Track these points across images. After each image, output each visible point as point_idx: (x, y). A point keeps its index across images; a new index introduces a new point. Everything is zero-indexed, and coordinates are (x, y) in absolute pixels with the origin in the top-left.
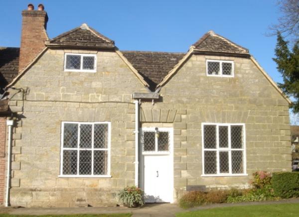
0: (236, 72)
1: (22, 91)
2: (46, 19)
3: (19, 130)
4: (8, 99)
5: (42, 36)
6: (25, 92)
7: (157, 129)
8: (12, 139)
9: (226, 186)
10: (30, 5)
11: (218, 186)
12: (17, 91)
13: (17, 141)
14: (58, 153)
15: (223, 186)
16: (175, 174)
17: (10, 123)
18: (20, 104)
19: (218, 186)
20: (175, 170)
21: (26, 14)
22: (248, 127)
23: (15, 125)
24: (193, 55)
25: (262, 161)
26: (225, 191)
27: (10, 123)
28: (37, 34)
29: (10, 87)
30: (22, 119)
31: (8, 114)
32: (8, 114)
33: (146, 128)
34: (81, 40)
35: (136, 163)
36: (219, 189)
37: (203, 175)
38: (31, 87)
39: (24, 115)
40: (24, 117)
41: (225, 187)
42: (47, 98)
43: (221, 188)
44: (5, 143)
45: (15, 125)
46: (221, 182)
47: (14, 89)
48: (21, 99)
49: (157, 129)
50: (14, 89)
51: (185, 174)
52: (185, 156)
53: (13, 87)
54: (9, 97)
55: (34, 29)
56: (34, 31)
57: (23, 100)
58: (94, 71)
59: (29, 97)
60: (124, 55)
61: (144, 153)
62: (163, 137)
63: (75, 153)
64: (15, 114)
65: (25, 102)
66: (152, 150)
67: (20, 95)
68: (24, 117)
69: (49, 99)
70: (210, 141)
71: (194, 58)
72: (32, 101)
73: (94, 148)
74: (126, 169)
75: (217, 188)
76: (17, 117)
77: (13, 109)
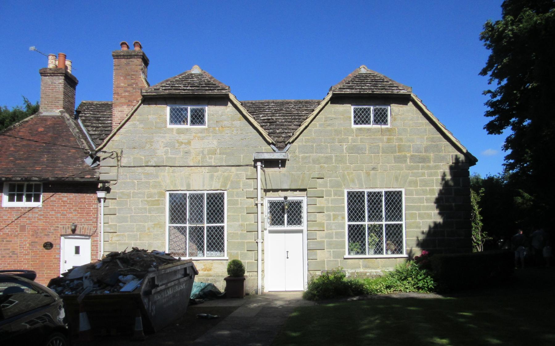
0: (394, 119)
1: (115, 155)
2: (146, 62)
5: (139, 83)
6: (118, 157)
7: (286, 198)
9: (379, 270)
10: (122, 44)
15: (373, 271)
21: (117, 57)
22: (408, 193)
28: (133, 81)
34: (187, 87)
36: (368, 274)
41: (376, 272)
42: (148, 162)
43: (371, 273)
44: (97, 220)
47: (105, 152)
49: (286, 198)
50: (105, 152)
55: (129, 75)
56: (128, 77)
58: (205, 127)
59: (124, 161)
60: (242, 105)
63: (202, 229)
66: (281, 224)
69: (150, 164)
70: (355, 212)
73: (208, 223)
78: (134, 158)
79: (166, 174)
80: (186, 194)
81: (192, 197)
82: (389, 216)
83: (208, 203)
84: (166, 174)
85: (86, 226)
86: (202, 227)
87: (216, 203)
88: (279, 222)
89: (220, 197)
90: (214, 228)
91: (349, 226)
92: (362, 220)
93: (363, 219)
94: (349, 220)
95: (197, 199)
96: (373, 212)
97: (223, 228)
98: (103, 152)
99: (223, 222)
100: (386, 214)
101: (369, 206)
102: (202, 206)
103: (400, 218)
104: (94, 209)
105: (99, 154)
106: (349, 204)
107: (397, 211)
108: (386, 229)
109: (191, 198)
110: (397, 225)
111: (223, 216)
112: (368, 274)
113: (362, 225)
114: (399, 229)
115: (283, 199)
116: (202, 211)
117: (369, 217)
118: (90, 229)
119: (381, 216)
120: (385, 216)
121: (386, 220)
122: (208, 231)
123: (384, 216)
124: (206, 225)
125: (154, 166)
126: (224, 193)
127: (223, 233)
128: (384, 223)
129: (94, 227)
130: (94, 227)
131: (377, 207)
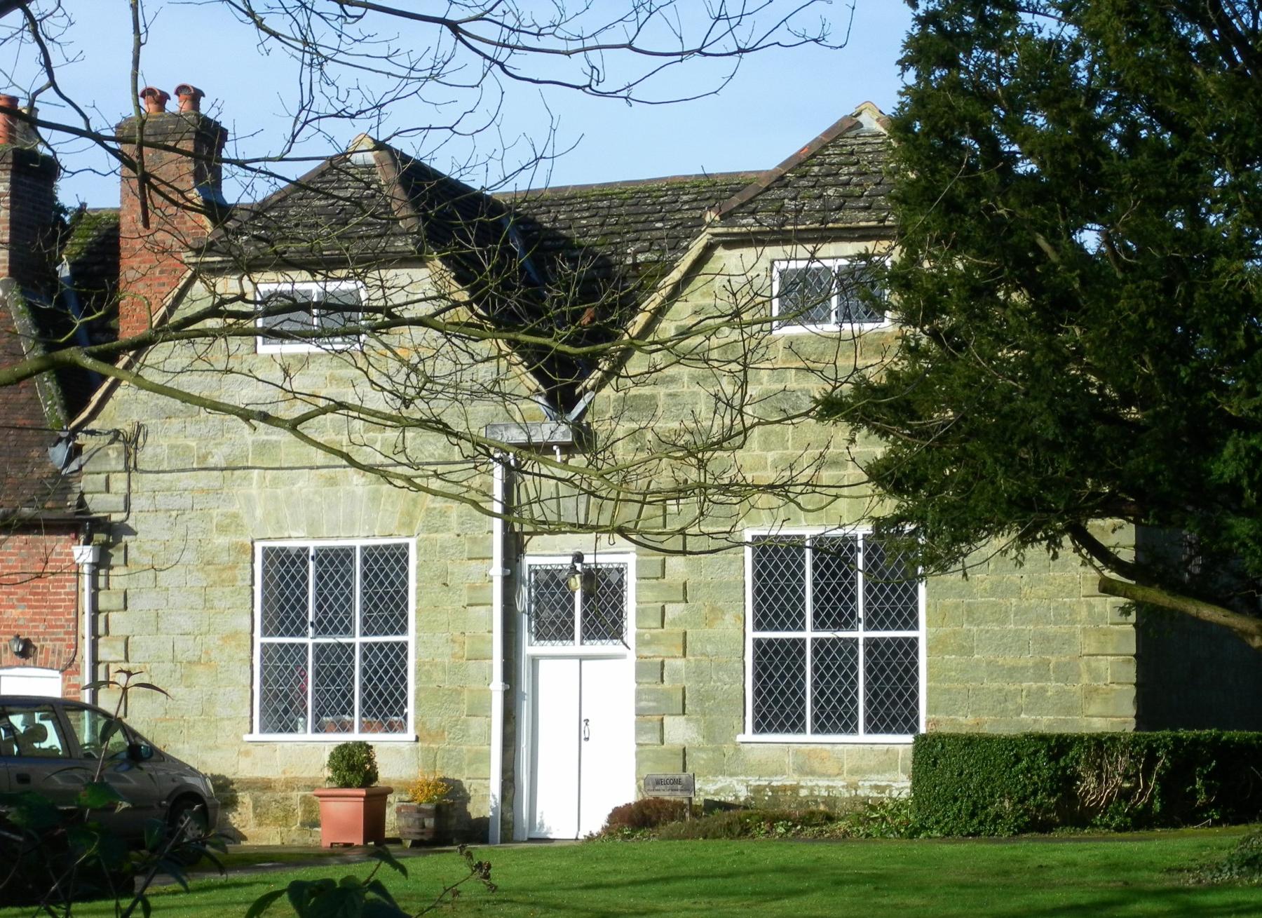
3: (118, 578)
4: (81, 467)
8: (95, 610)
9: (839, 783)
11: (807, 781)
12: (107, 439)
13: (112, 616)
14: (245, 655)
15: (823, 783)
16: (640, 730)
17: (84, 554)
18: (119, 483)
19: (807, 781)
20: (640, 713)
23: (102, 562)
24: (720, 252)
25: (995, 685)
26: (831, 801)
27: (84, 554)
29: (78, 428)
30: (125, 538)
31: (82, 524)
32: (82, 524)
33: (545, 554)
35: (497, 686)
36: (803, 793)
37: (749, 735)
38: (150, 423)
39: (130, 523)
40: (132, 532)
42: (205, 457)
43: (812, 789)
45: (102, 562)
46: (817, 765)
47: (93, 433)
48: (121, 467)
49: (579, 557)
50: (93, 433)
51: (679, 731)
52: (680, 662)
53: (94, 425)
54: (84, 458)
57: (127, 469)
59: (145, 456)
61: (530, 647)
62: (603, 594)
64: (102, 525)
65: (133, 474)
67: (114, 454)
68: (132, 532)
69: (211, 462)
70: (775, 603)
71: (728, 259)
72: (158, 472)
74: (465, 707)
75: (795, 789)
76: (106, 534)
77: (99, 504)
78: (171, 447)
79: (254, 491)
80: (305, 549)
81: (324, 556)
82: (876, 614)
83: (365, 576)
84: (254, 491)
85: (49, 645)
86: (350, 645)
87: (387, 576)
88: (559, 630)
89: (398, 556)
90: (381, 647)
91: (758, 643)
92: (794, 624)
93: (798, 624)
94: (758, 626)
95: (335, 561)
96: (828, 599)
97: (403, 647)
98: (87, 432)
99: (403, 630)
100: (868, 607)
101: (815, 584)
102: (348, 584)
103: (910, 621)
104: (67, 594)
105: (82, 438)
106: (758, 575)
107: (900, 598)
108: (869, 654)
109: (320, 563)
110: (900, 642)
111: (404, 614)
112: (803, 793)
113: (795, 642)
114: (906, 654)
115: (569, 560)
116: (348, 600)
117: (816, 615)
118: (60, 653)
119: (853, 614)
120: (866, 614)
121: (869, 625)
122: (365, 657)
123: (861, 614)
124: (358, 640)
125: (222, 469)
126: (407, 546)
127: (404, 664)
128: (861, 634)
129: (69, 646)
130: (69, 646)
131: (840, 585)
